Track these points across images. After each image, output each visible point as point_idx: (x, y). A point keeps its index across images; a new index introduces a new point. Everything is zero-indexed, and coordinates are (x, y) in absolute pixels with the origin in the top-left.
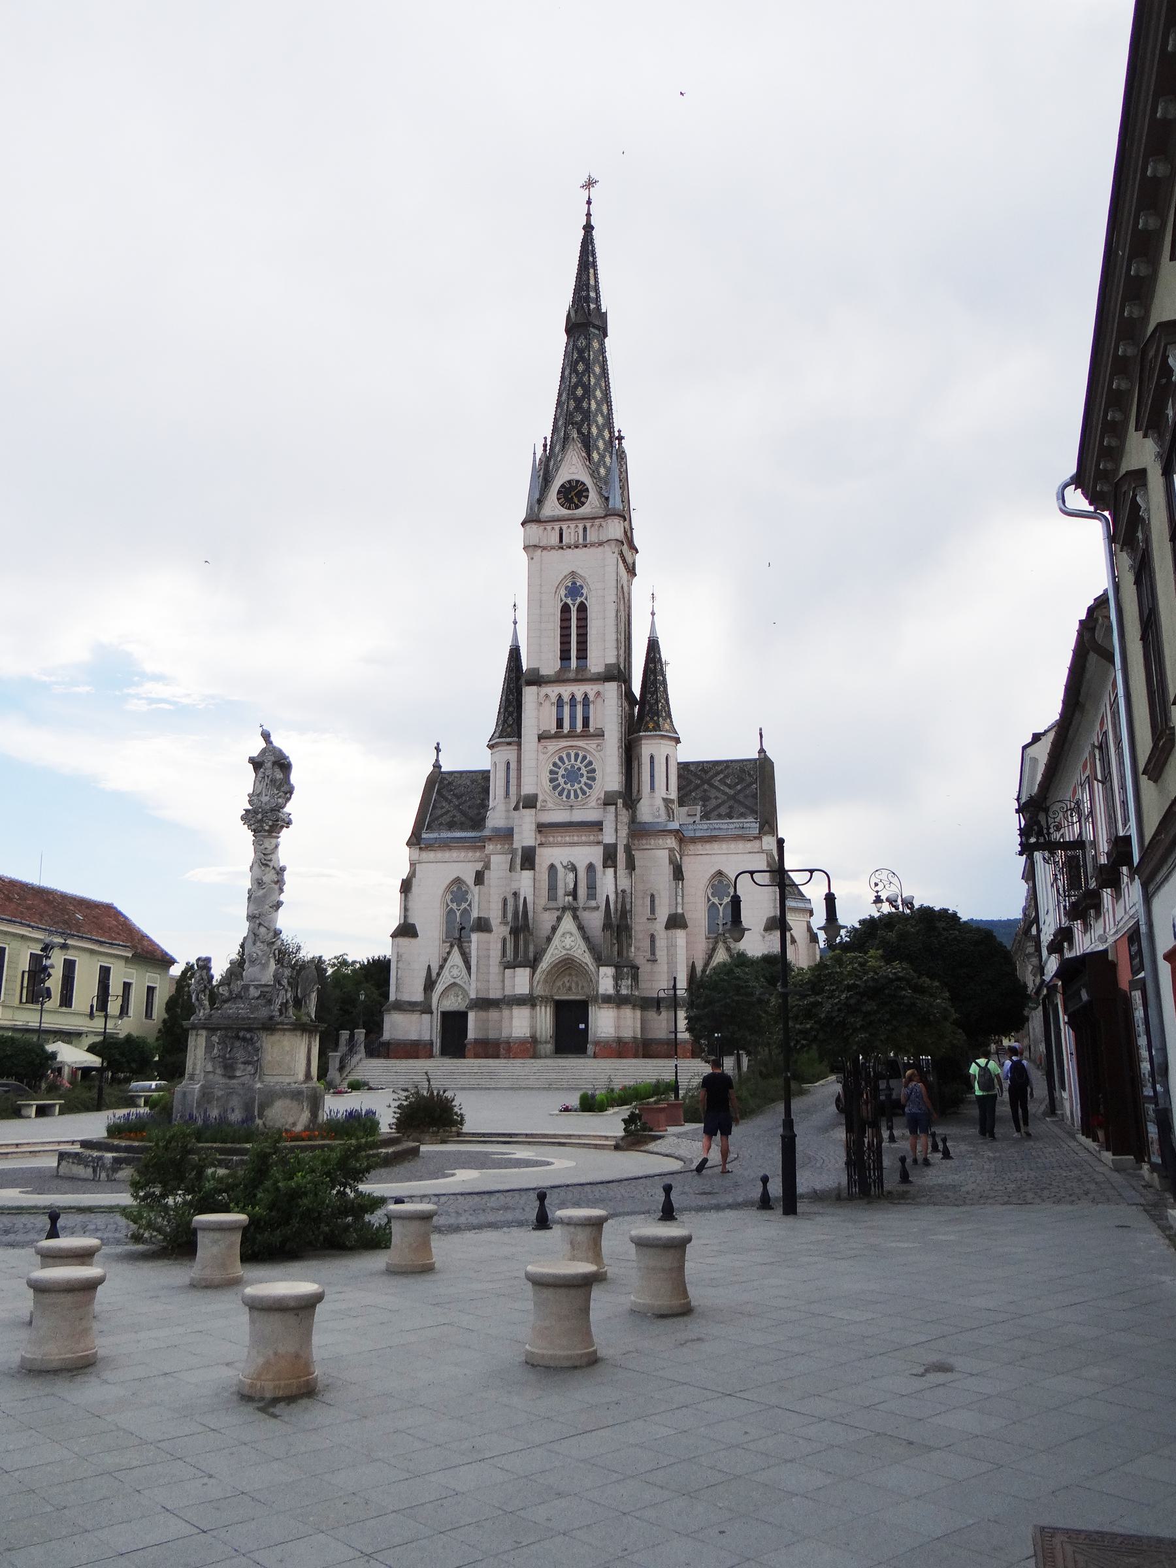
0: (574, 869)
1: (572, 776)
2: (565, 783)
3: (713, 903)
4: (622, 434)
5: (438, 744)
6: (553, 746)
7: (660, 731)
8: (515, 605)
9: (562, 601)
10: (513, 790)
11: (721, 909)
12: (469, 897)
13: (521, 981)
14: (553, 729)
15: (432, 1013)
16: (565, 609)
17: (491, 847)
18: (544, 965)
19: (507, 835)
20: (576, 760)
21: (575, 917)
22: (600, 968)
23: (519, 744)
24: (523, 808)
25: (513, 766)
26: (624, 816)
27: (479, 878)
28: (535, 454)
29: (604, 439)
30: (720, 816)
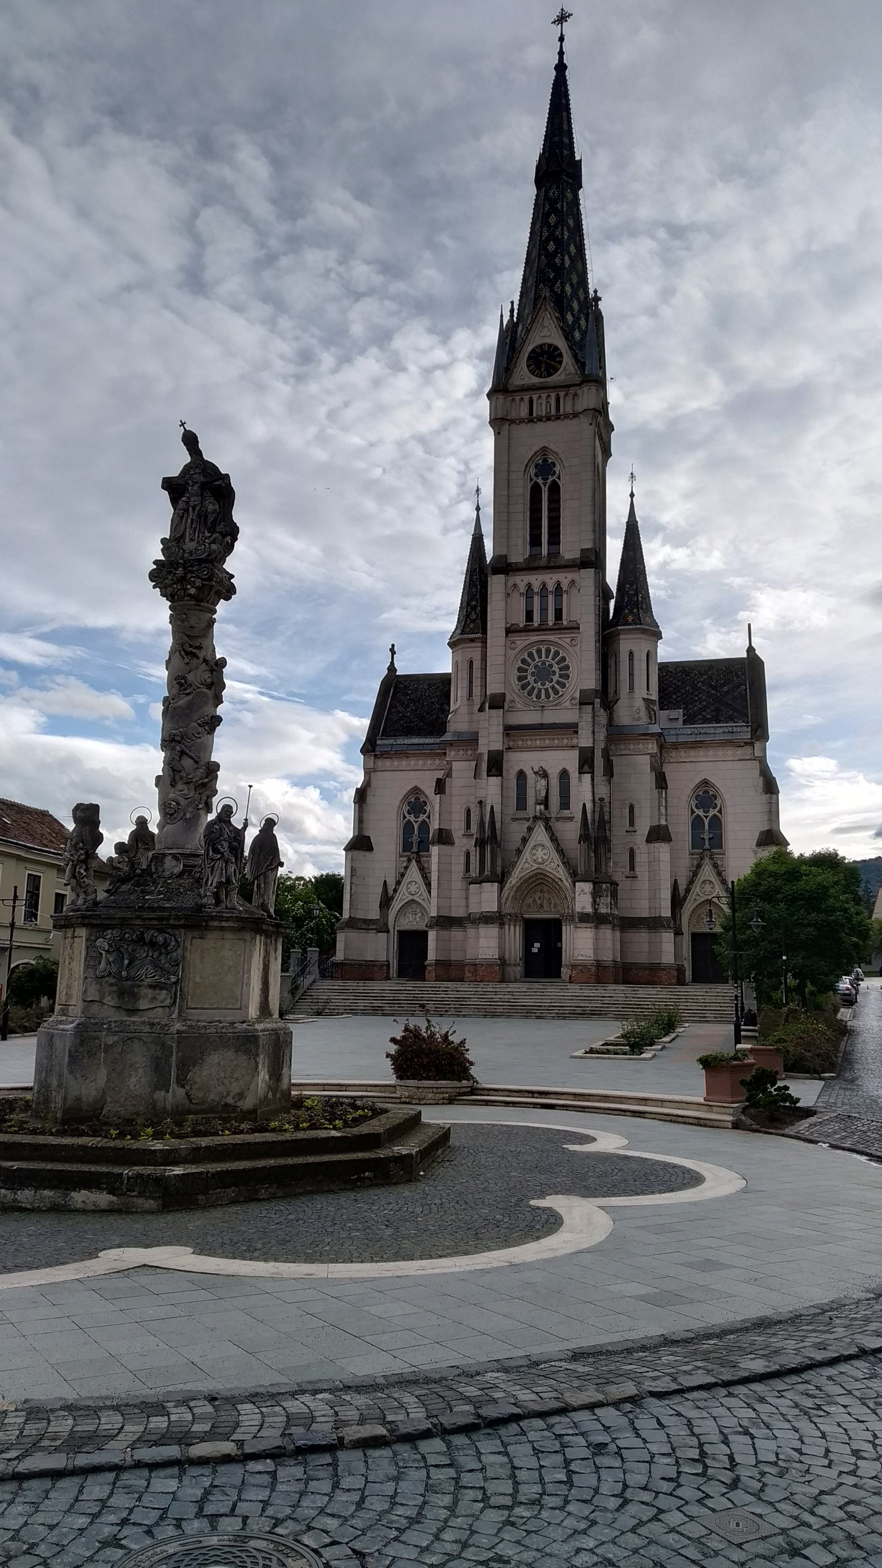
0: (544, 775)
1: (544, 673)
2: (535, 681)
3: (698, 816)
4: (599, 294)
5: (393, 646)
6: (522, 641)
7: (641, 624)
8: (478, 490)
9: (531, 480)
10: (477, 690)
11: (706, 822)
12: (428, 808)
14: (521, 622)
15: (388, 932)
16: (536, 491)
17: (453, 753)
18: (513, 880)
19: (471, 740)
20: (547, 657)
21: (548, 828)
22: (577, 884)
23: (484, 642)
24: (490, 708)
25: (477, 665)
26: (603, 717)
27: (440, 786)
28: (502, 316)
29: (578, 300)
30: (705, 721)
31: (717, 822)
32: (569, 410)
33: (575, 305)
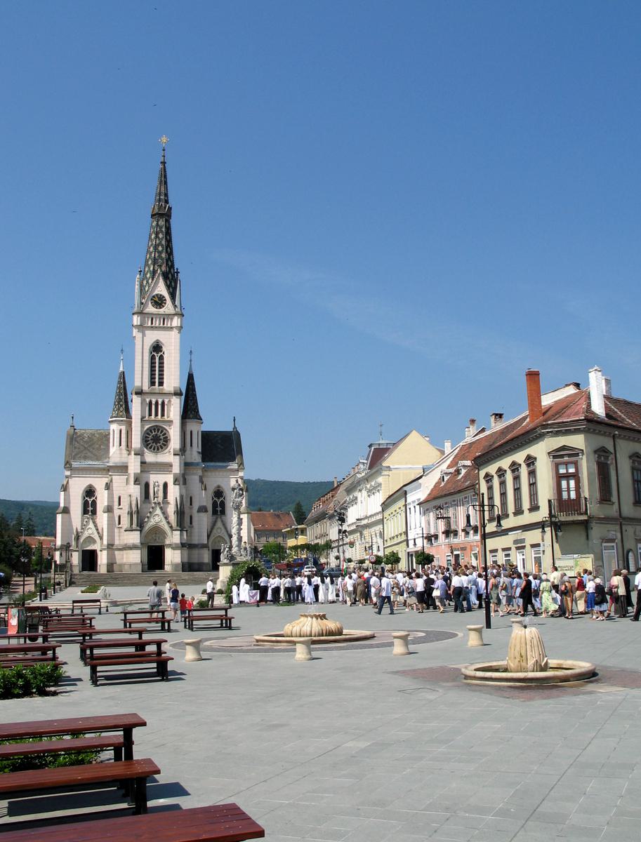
1: (156, 439)
13: (135, 538)
16: (153, 358)
18: (147, 527)
27: (108, 487)
31: (223, 504)
32: (169, 325)
33: (170, 276)
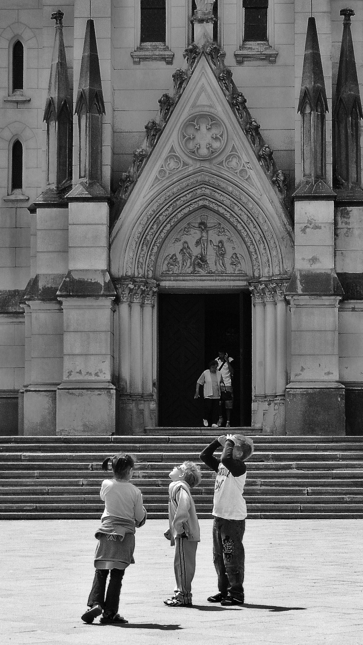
22: (299, 206)
